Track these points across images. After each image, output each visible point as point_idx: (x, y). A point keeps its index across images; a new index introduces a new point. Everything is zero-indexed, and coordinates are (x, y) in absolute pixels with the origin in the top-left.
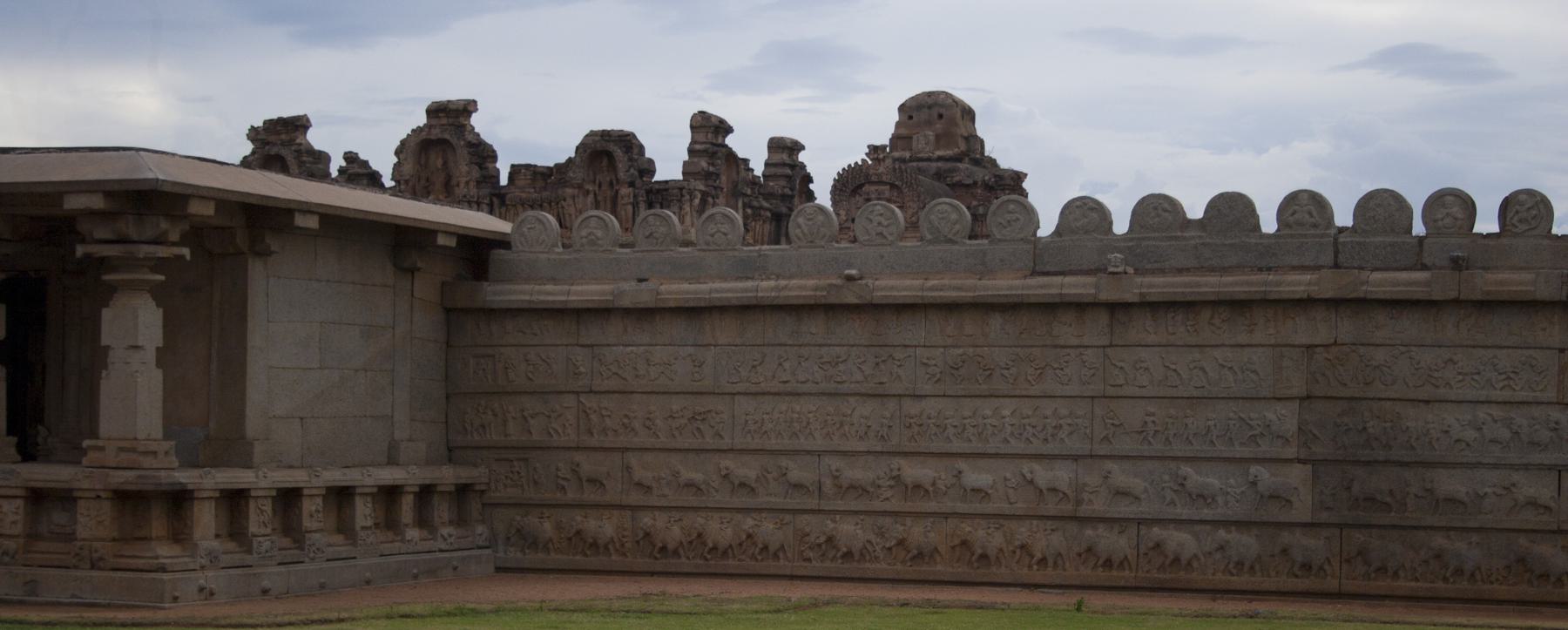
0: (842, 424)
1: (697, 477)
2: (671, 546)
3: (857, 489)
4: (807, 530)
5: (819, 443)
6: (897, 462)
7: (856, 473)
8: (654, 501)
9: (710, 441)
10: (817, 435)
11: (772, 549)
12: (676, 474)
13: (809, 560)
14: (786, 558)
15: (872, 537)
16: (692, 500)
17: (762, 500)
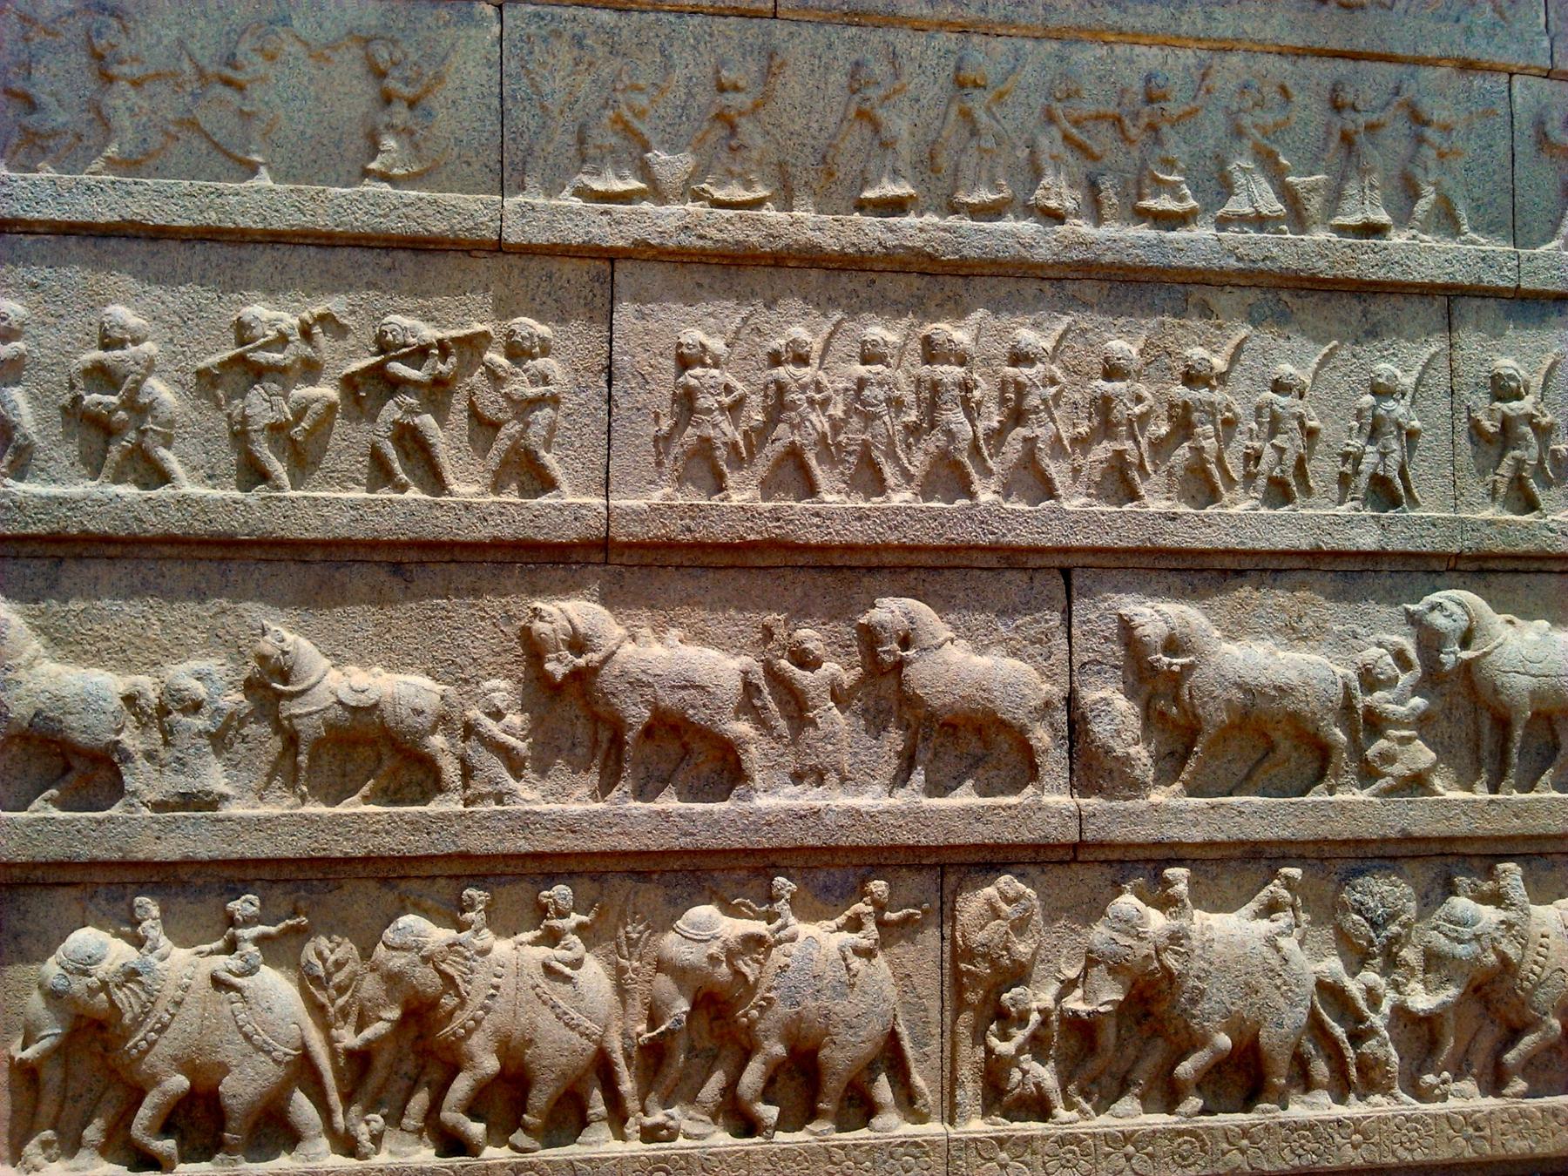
0: (1183, 423)
1: (405, 689)
2: (243, 1085)
3: (1278, 742)
4: (1023, 948)
5: (1077, 512)
6: (1453, 604)
7: (1255, 653)
8: (132, 827)
9: (471, 496)
10: (1057, 470)
11: (840, 1057)
12: (269, 684)
13: (1038, 1107)
14: (908, 1101)
15: (1332, 966)
16: (362, 818)
17: (773, 801)
